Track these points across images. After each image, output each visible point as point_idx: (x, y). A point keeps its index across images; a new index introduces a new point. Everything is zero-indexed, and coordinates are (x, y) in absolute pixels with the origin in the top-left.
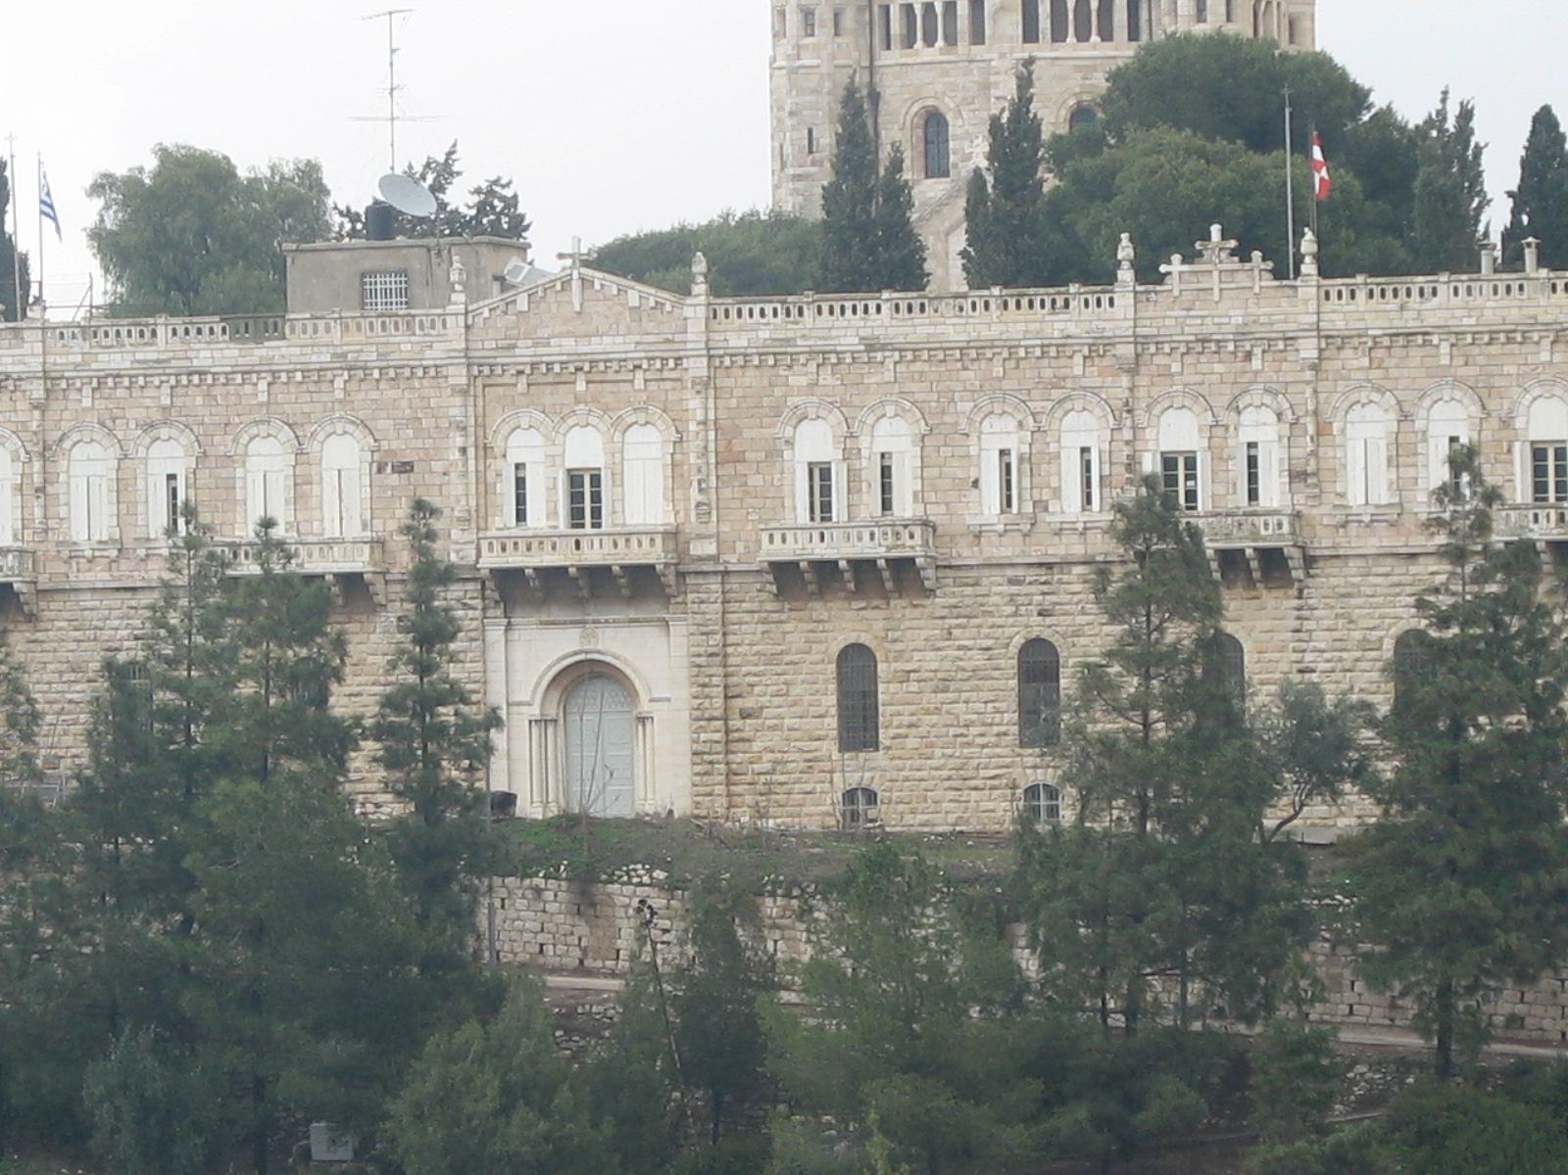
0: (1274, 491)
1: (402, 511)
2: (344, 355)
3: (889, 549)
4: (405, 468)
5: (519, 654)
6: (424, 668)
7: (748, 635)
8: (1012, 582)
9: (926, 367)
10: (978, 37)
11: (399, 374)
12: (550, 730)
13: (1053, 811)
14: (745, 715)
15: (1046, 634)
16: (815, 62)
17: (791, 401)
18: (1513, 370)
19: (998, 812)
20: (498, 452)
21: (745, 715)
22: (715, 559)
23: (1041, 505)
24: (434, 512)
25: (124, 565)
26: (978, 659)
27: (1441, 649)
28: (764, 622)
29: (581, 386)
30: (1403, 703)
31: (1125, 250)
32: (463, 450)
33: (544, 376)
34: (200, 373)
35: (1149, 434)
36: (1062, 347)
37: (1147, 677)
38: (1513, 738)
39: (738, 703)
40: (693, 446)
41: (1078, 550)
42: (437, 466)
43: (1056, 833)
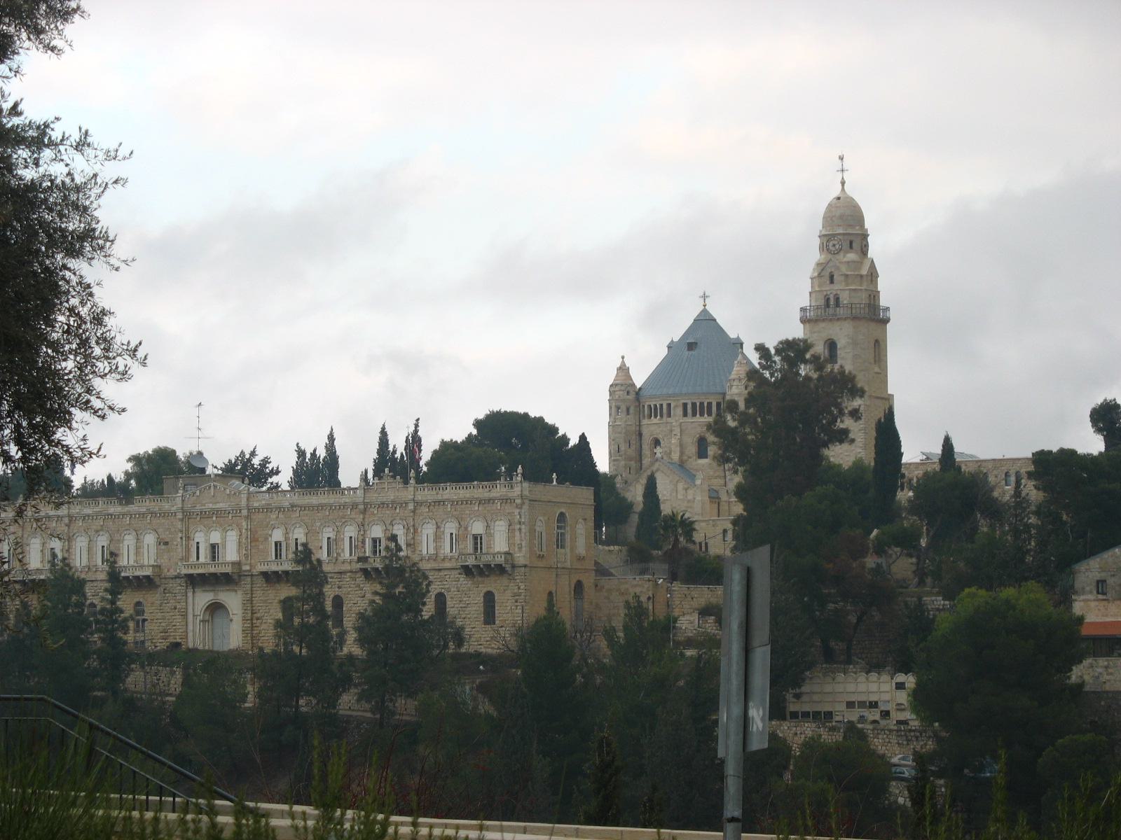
2: (149, 510)
3: (292, 568)
5: (197, 599)
7: (258, 594)
9: (309, 512)
10: (669, 415)
11: (165, 515)
12: (207, 624)
14: (258, 619)
15: (340, 594)
16: (620, 423)
17: (271, 523)
18: (468, 512)
20: (192, 538)
21: (258, 619)
22: (250, 571)
23: (338, 554)
25: (90, 573)
28: (263, 590)
29: (214, 518)
32: (181, 538)
33: (205, 515)
34: (111, 515)
35: (368, 532)
36: (345, 506)
39: (255, 615)
40: (244, 536)
41: (349, 568)
42: (175, 543)
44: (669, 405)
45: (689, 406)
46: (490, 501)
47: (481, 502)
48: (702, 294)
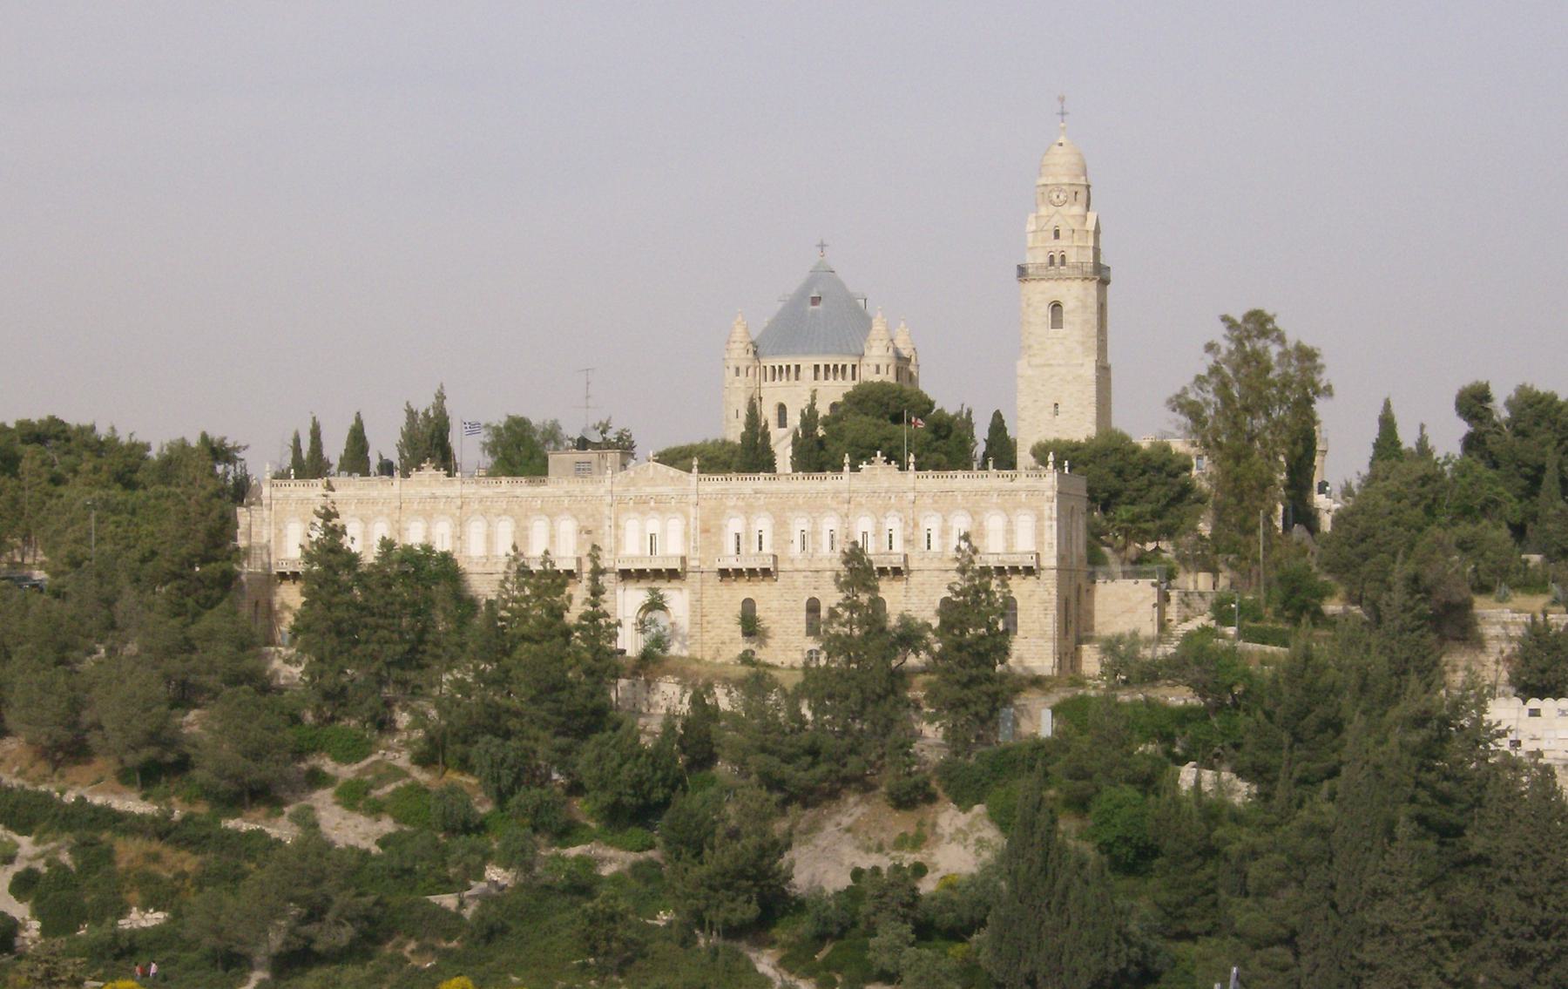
0: (898, 546)
1: (588, 548)
4: (589, 532)
6: (595, 605)
8: (805, 577)
13: (818, 659)
14: (708, 623)
19: (798, 659)
21: (708, 623)
24: (599, 549)
26: (793, 604)
27: (957, 604)
29: (652, 504)
30: (943, 623)
31: (847, 460)
37: (852, 613)
38: (982, 637)
43: (818, 667)
44: (798, 367)
45: (822, 369)
46: (1013, 492)
47: (1000, 493)
48: (819, 242)
